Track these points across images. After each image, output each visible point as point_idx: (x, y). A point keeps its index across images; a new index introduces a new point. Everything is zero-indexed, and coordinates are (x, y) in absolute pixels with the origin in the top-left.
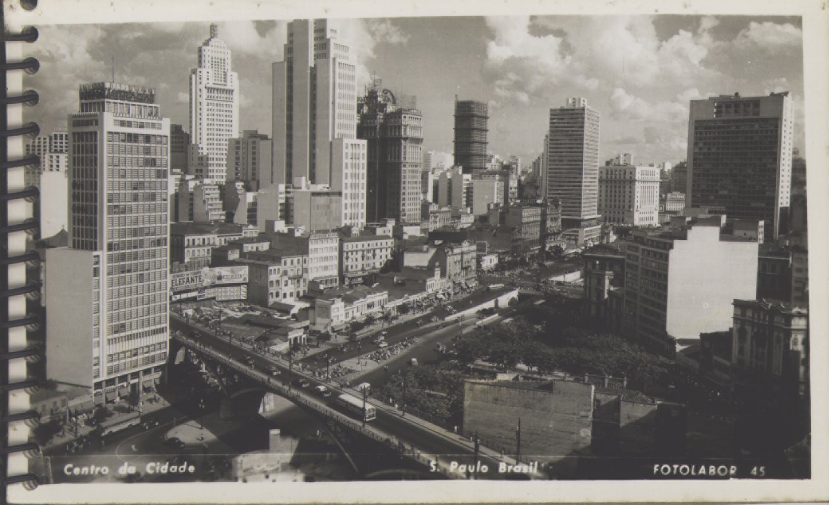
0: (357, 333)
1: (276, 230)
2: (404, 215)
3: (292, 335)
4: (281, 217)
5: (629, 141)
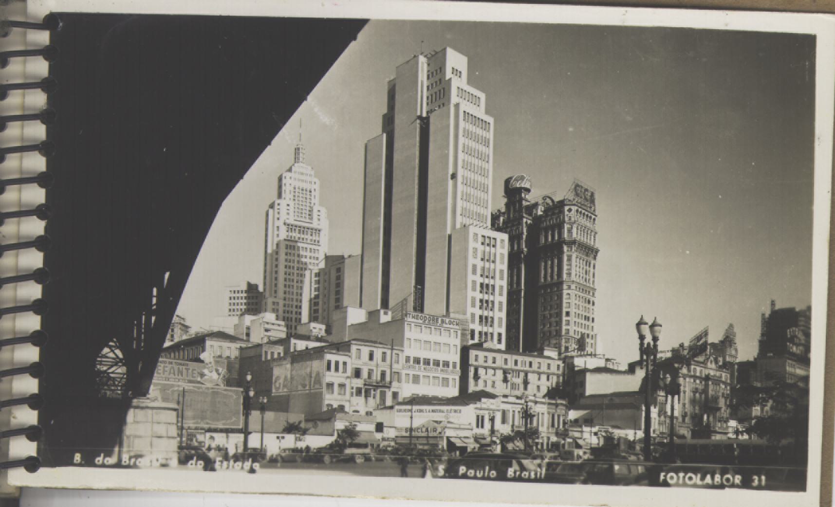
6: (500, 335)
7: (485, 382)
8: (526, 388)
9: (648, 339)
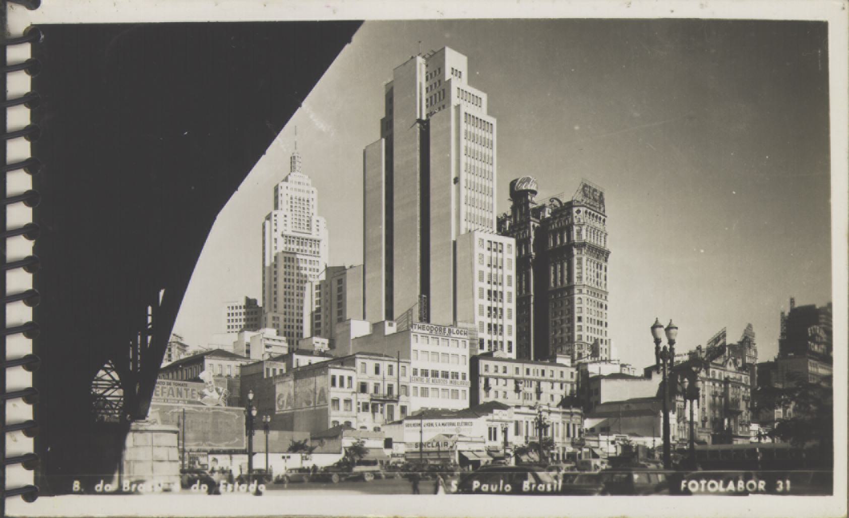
6: (510, 343)
7: (496, 392)
8: (538, 398)
9: (664, 342)
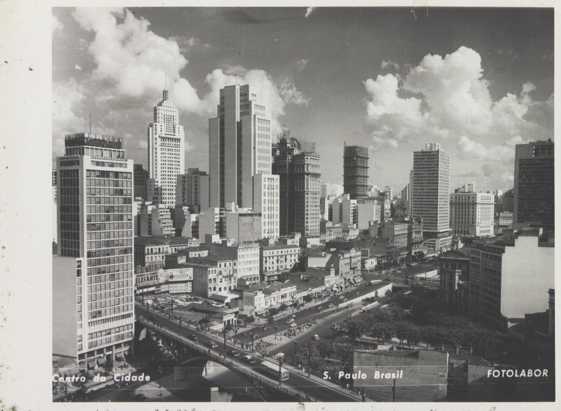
0: (274, 317)
1: (213, 242)
2: (308, 230)
3: (225, 319)
4: (216, 232)
5: (472, 175)
8: (286, 261)
